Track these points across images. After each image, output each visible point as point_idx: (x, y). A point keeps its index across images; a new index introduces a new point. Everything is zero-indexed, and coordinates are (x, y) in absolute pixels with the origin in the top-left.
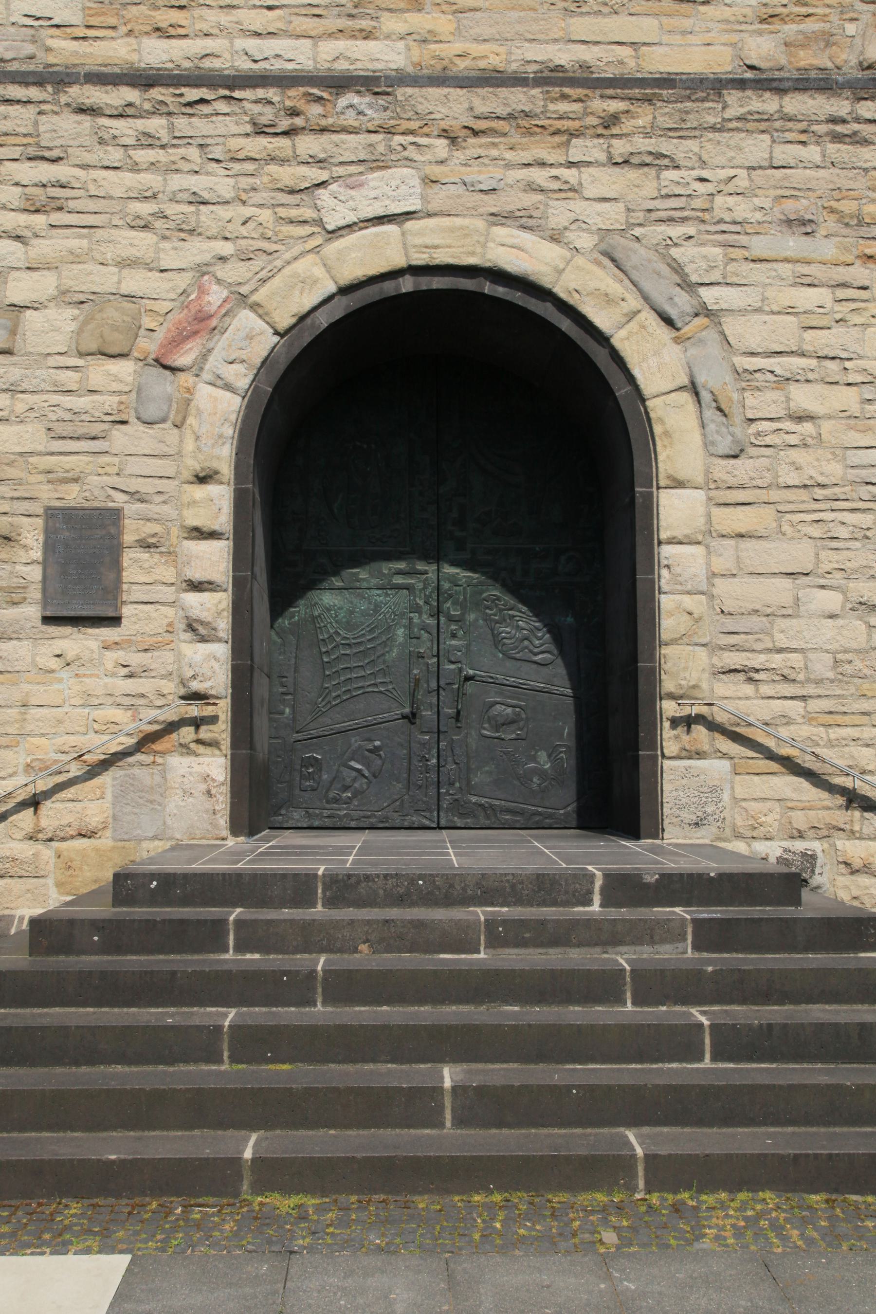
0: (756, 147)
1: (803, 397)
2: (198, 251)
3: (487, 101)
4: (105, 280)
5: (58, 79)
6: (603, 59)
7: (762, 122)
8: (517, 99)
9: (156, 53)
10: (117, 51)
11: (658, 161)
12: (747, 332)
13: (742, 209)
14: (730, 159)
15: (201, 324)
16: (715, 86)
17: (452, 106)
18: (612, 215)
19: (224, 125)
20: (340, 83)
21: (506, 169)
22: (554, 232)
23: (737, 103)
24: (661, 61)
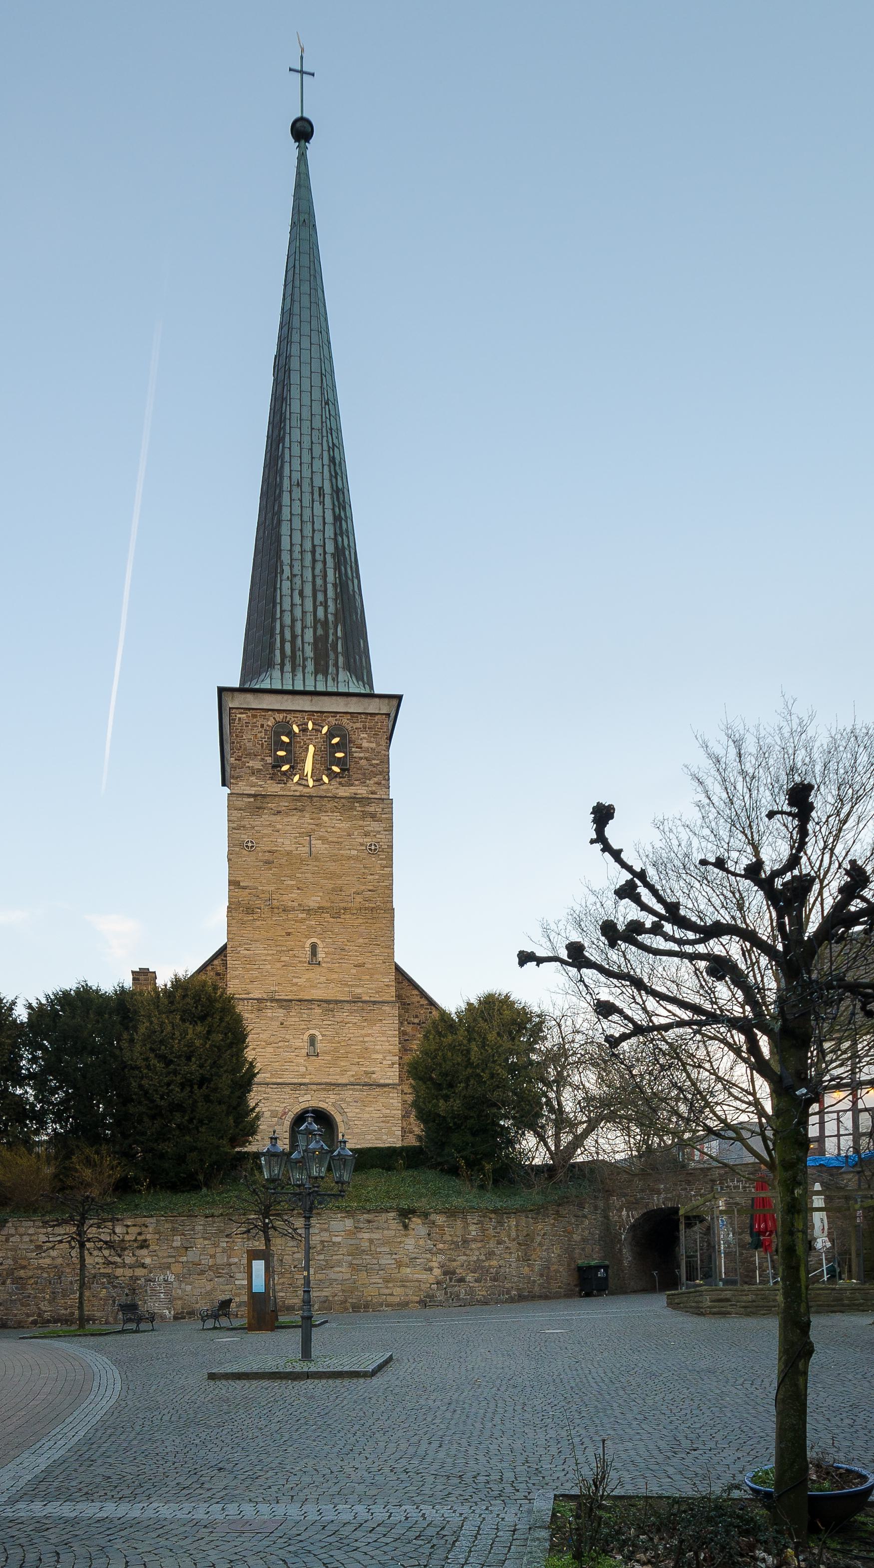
0: (351, 1092)
1: (356, 1122)
2: (285, 1105)
3: (318, 1087)
4: (273, 1108)
5: (268, 1084)
6: (333, 1081)
7: (352, 1089)
8: (323, 1086)
9: (279, 1081)
10: (274, 1080)
11: (339, 1094)
12: (349, 1115)
13: (349, 1100)
14: (348, 1094)
15: (285, 1113)
16: (346, 1085)
17: (314, 1087)
18: (334, 1101)
19: (287, 1089)
20: (301, 1084)
21: (322, 1095)
22: (326, 1102)
23: (349, 1087)
24: (340, 1081)
